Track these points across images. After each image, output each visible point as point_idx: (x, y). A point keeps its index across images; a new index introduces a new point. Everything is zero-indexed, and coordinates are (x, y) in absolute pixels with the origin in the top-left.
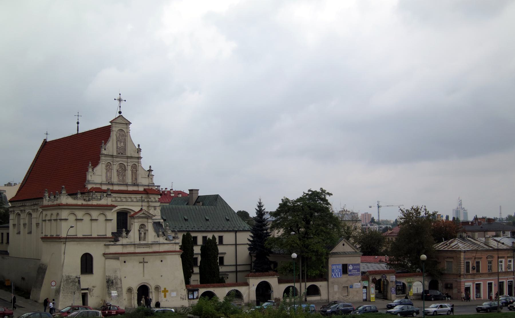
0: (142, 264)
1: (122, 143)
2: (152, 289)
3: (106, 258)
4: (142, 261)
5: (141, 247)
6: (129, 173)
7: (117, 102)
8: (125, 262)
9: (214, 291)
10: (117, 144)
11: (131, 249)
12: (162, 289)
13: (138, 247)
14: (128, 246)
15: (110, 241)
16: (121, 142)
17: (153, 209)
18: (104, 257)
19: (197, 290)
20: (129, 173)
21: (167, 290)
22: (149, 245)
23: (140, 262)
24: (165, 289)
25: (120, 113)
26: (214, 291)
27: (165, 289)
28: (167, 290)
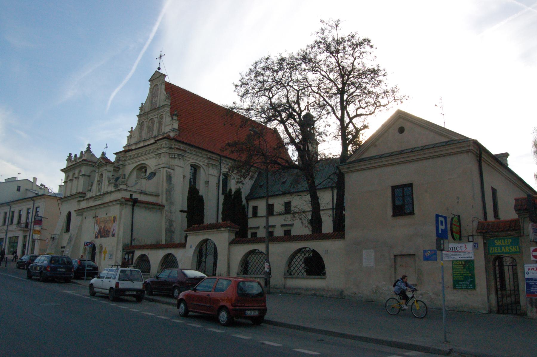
0: (94, 219)
1: (156, 98)
2: (97, 251)
3: (77, 215)
4: (94, 216)
5: (97, 199)
6: (156, 125)
7: (158, 60)
8: (86, 218)
9: (148, 254)
10: (152, 101)
11: (92, 203)
12: (104, 249)
13: (96, 200)
14: (90, 200)
15: (81, 197)
16: (155, 97)
17: (158, 158)
18: (76, 213)
19: (133, 253)
20: (156, 125)
21: (106, 250)
22: (101, 196)
23: (94, 217)
24: (105, 249)
25: (159, 69)
26: (148, 254)
27: (105, 249)
28: (106, 250)
